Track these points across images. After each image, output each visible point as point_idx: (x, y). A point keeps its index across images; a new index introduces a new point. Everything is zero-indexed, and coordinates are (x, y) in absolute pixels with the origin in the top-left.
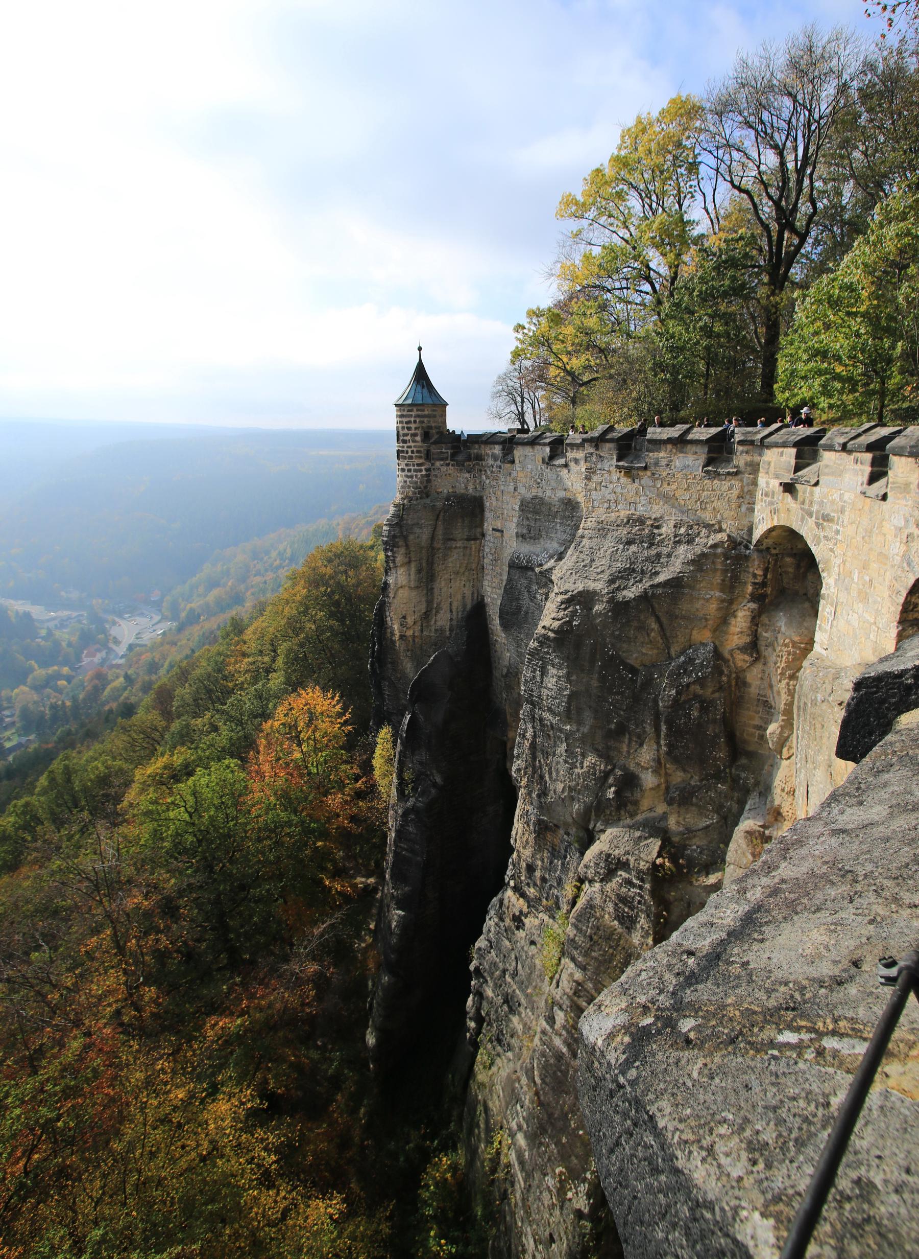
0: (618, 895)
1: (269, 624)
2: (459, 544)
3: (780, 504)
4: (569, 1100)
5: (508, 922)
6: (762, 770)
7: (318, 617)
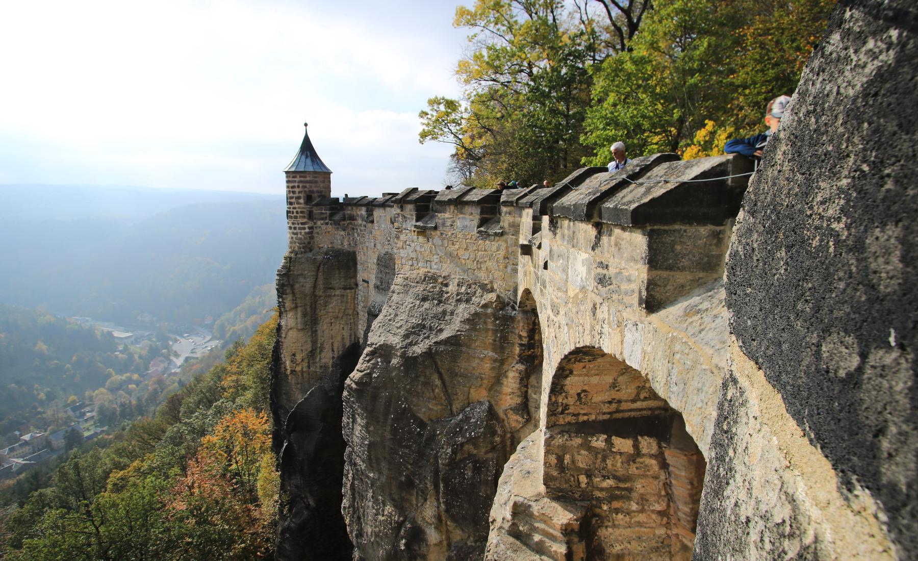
2: (338, 292)
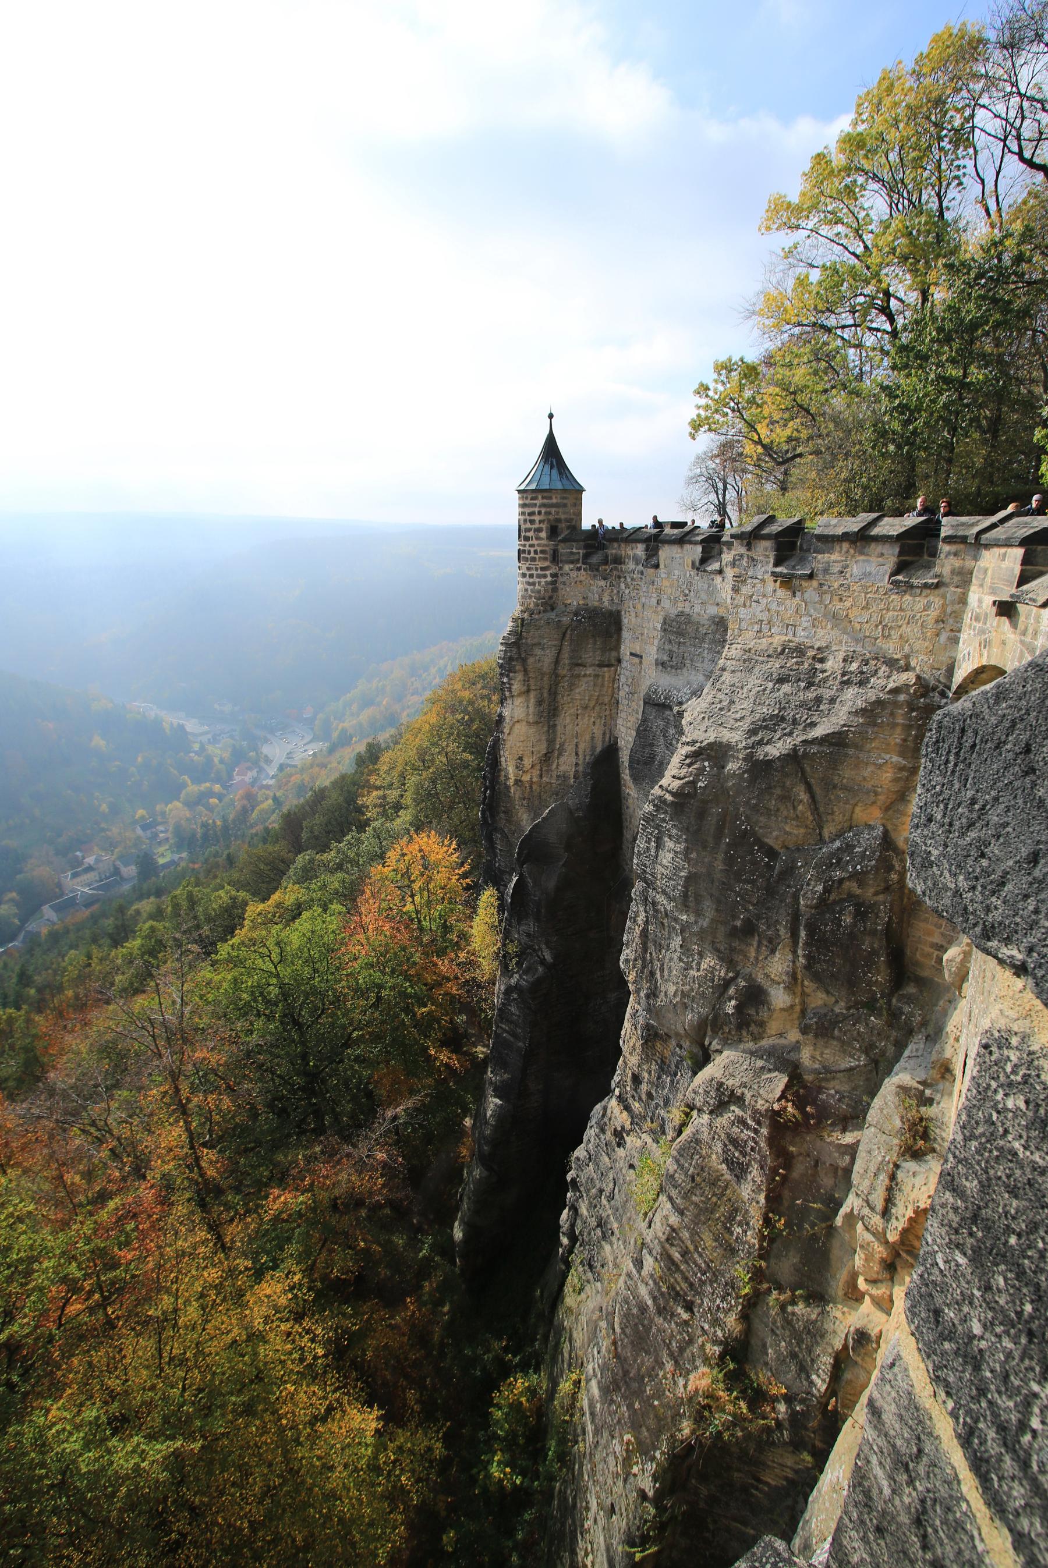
0: (728, 1135)
1: (405, 754)
2: (589, 671)
3: (994, 634)
4: (648, 1361)
5: (609, 1135)
6: (936, 1005)
7: (450, 749)
